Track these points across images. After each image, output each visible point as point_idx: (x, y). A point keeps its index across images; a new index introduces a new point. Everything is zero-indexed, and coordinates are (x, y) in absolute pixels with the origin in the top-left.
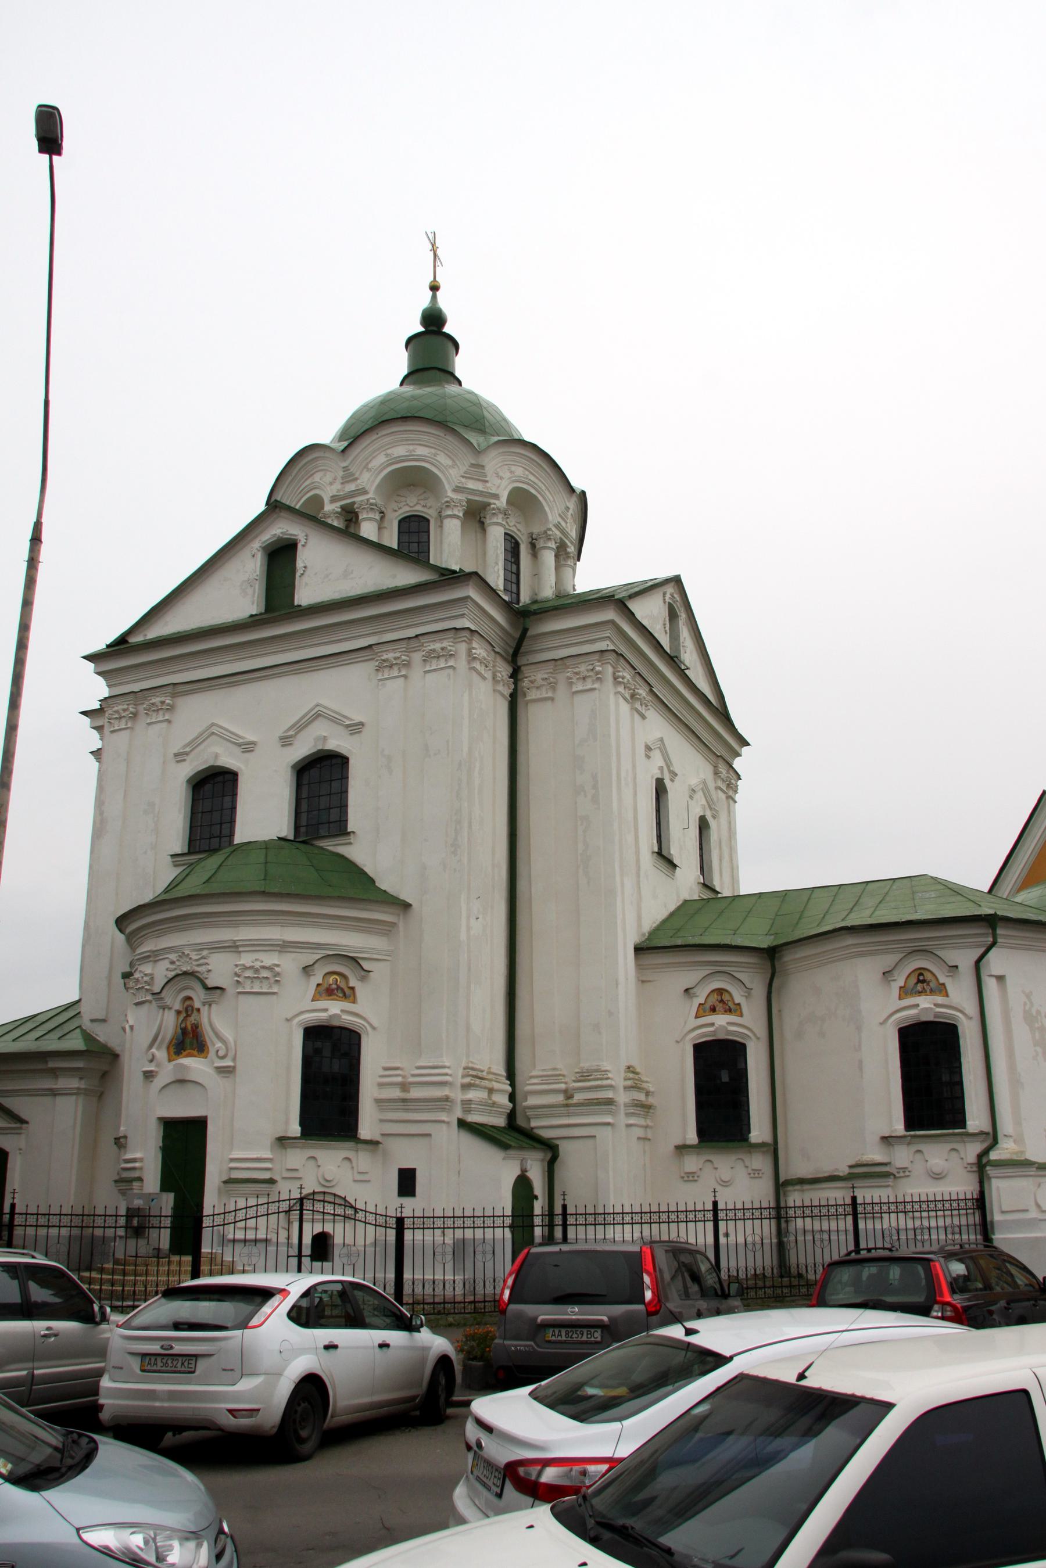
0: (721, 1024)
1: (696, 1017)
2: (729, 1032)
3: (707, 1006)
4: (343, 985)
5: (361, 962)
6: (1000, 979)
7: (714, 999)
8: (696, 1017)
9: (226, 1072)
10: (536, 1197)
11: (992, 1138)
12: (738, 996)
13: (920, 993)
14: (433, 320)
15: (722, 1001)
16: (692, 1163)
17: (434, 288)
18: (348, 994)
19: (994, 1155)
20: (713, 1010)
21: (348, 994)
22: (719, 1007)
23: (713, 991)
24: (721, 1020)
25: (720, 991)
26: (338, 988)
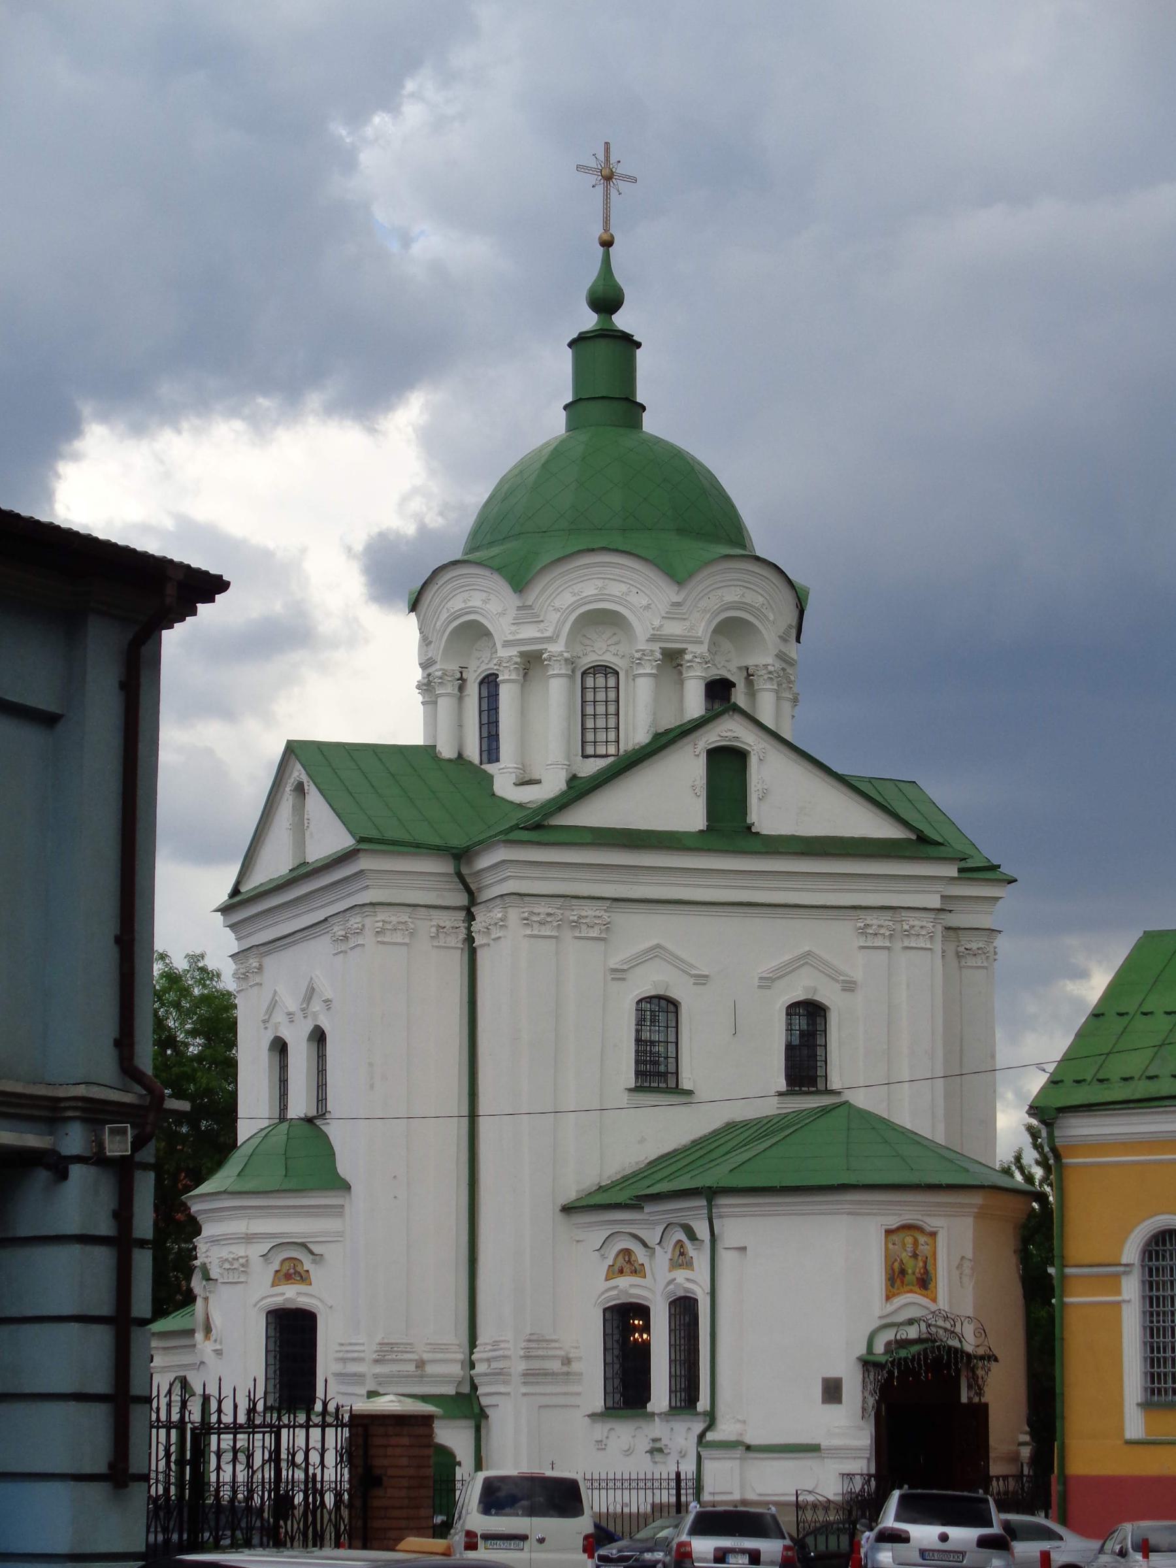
0: (628, 1288)
1: (607, 1279)
2: (632, 1296)
3: (616, 1268)
4: (299, 1269)
5: (311, 1246)
6: (743, 1249)
7: (620, 1261)
8: (607, 1279)
9: (218, 1353)
10: (459, 1464)
11: (711, 1419)
12: (640, 1255)
13: (681, 1266)
14: (606, 301)
15: (629, 1262)
16: (600, 1430)
17: (607, 244)
18: (303, 1278)
19: (710, 1436)
20: (621, 1272)
21: (303, 1278)
22: (627, 1268)
23: (622, 1250)
24: (624, 1282)
25: (627, 1252)
26: (296, 1272)
